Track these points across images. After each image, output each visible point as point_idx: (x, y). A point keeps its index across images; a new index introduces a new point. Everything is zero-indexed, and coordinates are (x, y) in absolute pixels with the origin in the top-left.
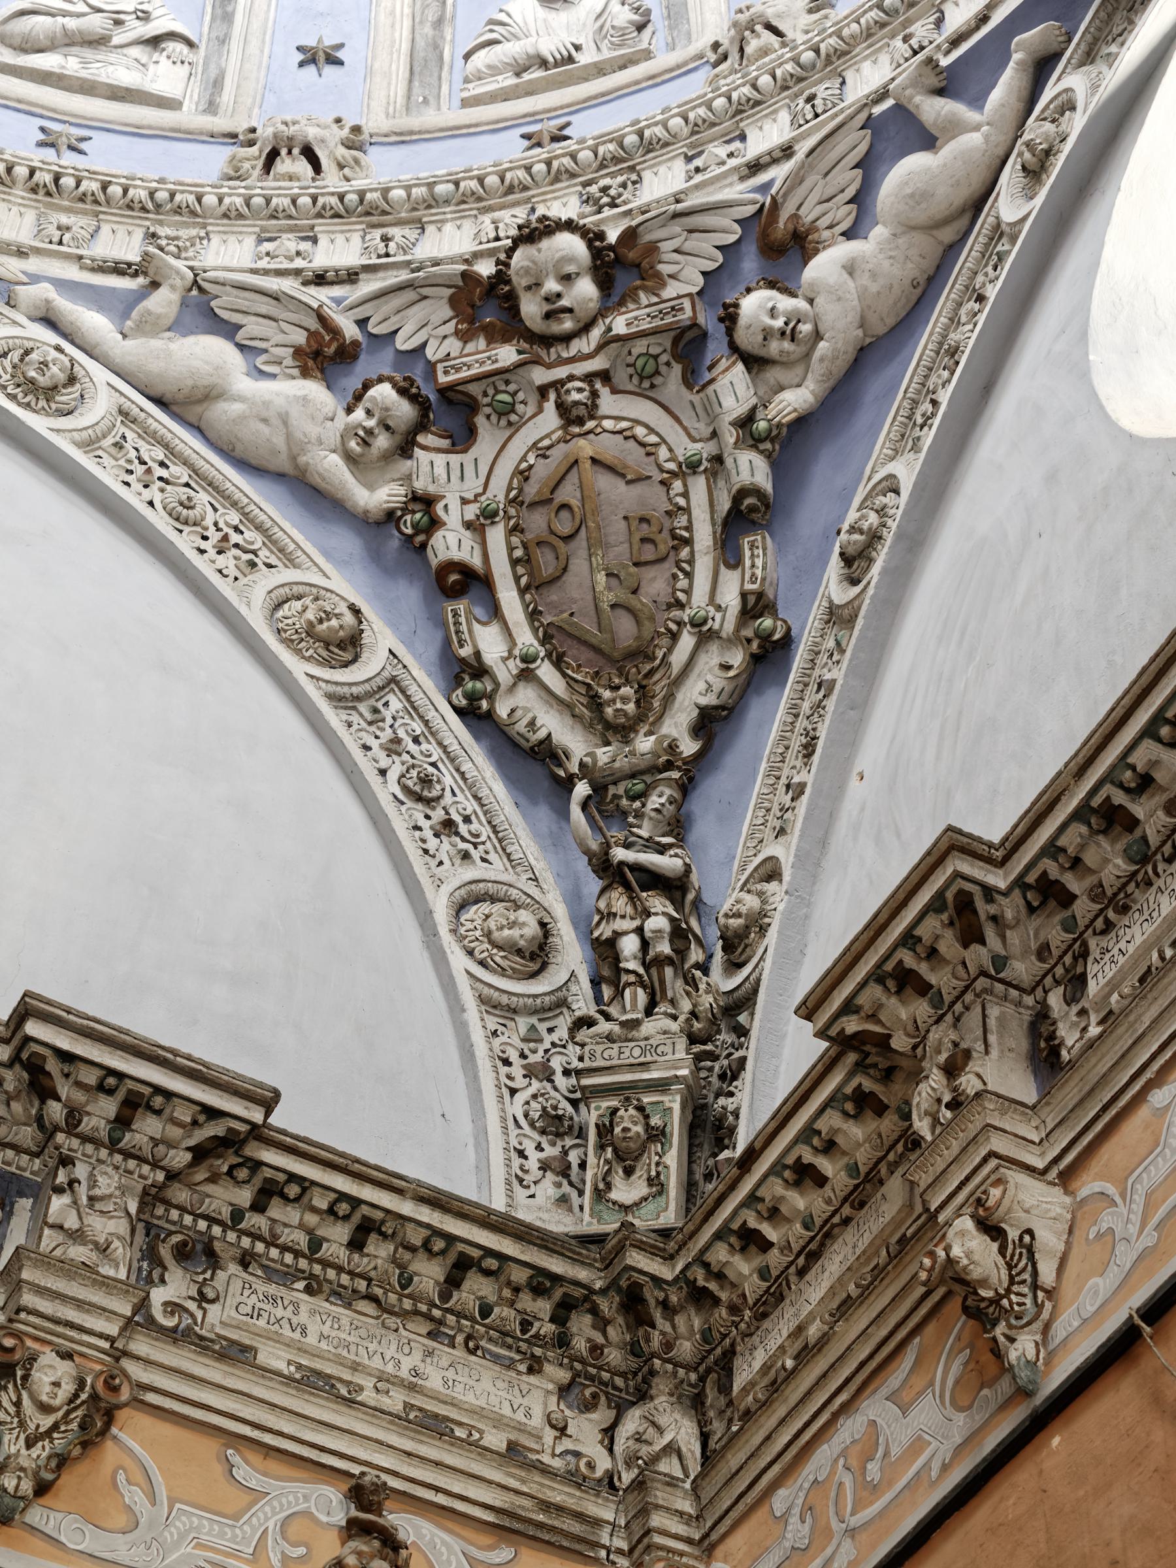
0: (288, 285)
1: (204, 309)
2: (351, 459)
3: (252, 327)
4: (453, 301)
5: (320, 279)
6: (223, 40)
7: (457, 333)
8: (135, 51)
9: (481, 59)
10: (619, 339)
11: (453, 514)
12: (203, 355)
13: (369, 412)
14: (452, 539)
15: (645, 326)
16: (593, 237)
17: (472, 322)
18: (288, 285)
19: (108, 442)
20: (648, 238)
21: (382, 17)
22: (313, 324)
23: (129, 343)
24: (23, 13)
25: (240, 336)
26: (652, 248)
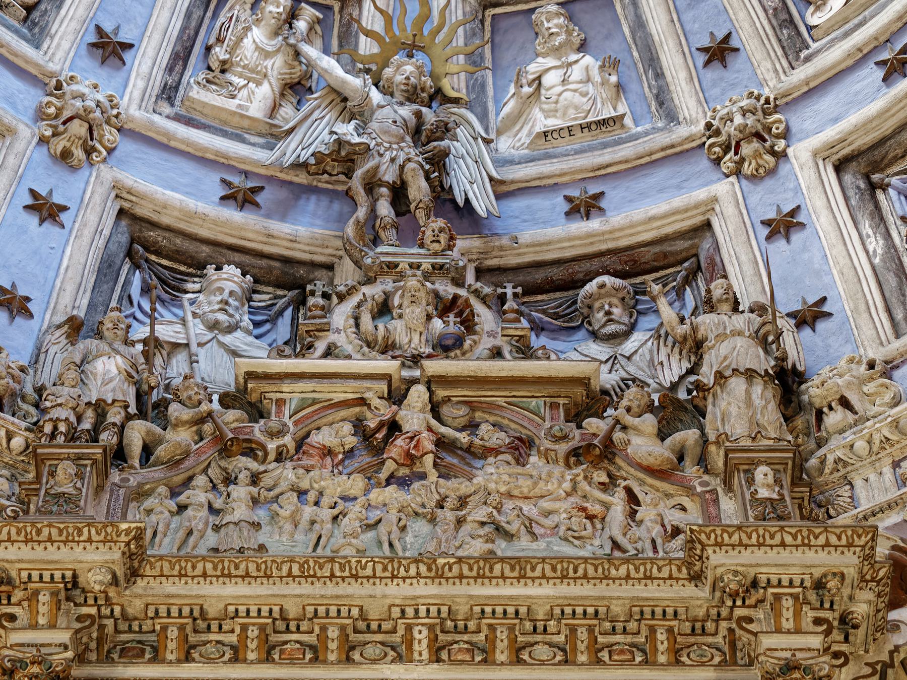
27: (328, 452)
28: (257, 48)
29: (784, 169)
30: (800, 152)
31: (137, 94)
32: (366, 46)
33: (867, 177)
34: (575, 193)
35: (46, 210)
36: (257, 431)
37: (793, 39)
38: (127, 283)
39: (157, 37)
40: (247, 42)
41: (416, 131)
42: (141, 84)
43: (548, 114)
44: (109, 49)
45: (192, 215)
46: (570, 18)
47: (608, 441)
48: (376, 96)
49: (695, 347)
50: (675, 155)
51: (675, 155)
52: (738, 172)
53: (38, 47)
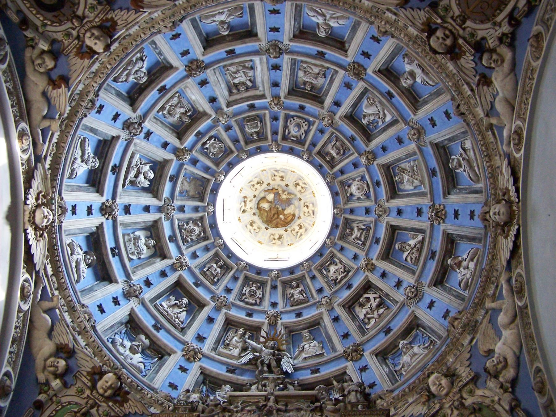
0: (477, 97)
1: (491, 112)
2: (503, 61)
3: (489, 99)
4: (459, 59)
5: (472, 90)
6: (456, 136)
7: (465, 55)
8: (468, 153)
9: (431, 83)
10: (442, 19)
11: (499, 31)
12: (499, 106)
13: (491, 64)
14: (504, 28)
15: (435, 15)
16: (429, 38)
17: (461, 53)
18: (477, 97)
19: (524, 117)
20: (422, 27)
21: (435, 107)
22: (481, 86)
23: (506, 123)
24: (471, 179)
25: (492, 100)
26: (423, 24)
27: (249, 411)
28: (236, 341)
29: (363, 358)
30: (366, 354)
31: (207, 348)
32: (262, 340)
33: (383, 357)
34: (313, 369)
35: (183, 369)
36: (232, 407)
37: (362, 331)
38: (202, 388)
39: (212, 336)
40: (234, 339)
41: (274, 355)
42: (208, 346)
43: (306, 354)
44: (200, 338)
45: (219, 374)
46: (310, 333)
47: (321, 407)
48: (264, 348)
49: (342, 390)
50: (337, 358)
51: (337, 358)
52: (352, 360)
53: (184, 336)
